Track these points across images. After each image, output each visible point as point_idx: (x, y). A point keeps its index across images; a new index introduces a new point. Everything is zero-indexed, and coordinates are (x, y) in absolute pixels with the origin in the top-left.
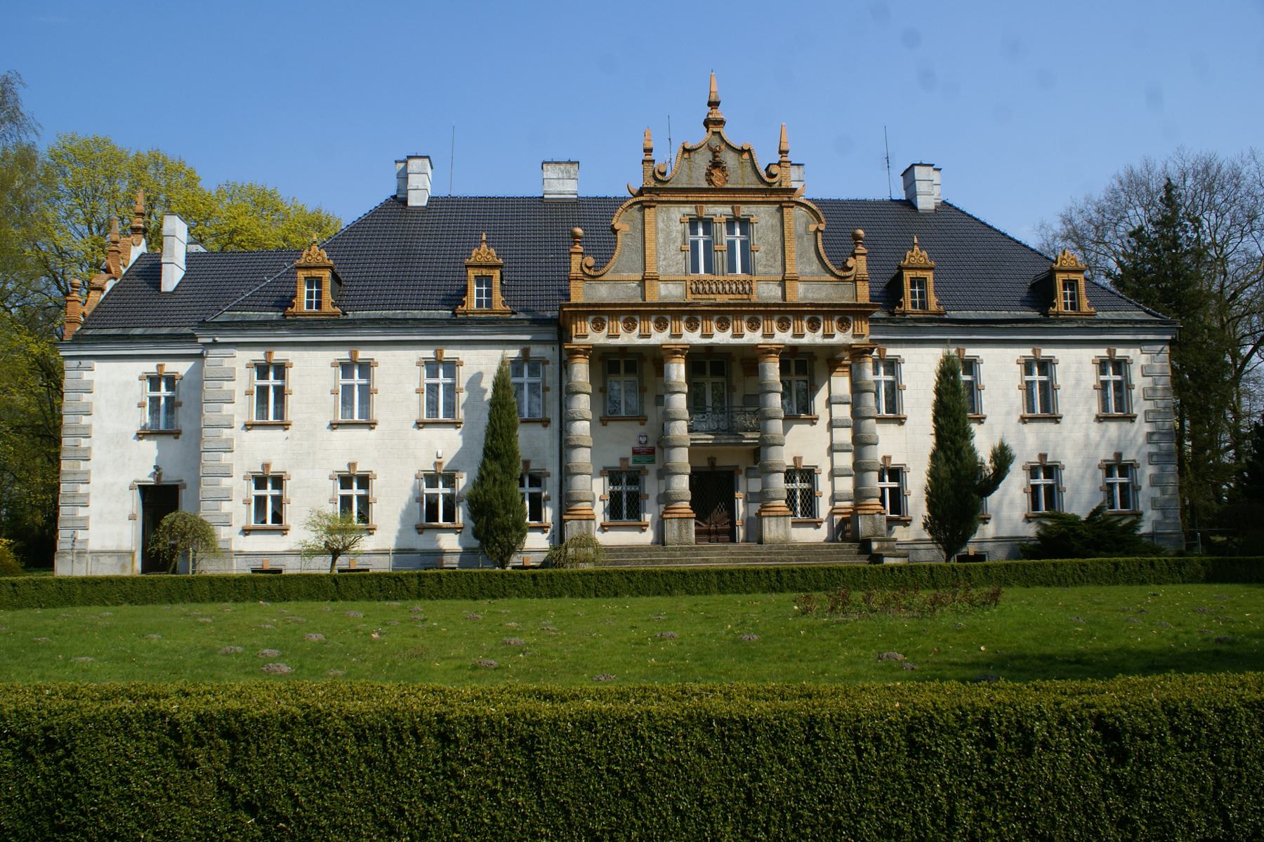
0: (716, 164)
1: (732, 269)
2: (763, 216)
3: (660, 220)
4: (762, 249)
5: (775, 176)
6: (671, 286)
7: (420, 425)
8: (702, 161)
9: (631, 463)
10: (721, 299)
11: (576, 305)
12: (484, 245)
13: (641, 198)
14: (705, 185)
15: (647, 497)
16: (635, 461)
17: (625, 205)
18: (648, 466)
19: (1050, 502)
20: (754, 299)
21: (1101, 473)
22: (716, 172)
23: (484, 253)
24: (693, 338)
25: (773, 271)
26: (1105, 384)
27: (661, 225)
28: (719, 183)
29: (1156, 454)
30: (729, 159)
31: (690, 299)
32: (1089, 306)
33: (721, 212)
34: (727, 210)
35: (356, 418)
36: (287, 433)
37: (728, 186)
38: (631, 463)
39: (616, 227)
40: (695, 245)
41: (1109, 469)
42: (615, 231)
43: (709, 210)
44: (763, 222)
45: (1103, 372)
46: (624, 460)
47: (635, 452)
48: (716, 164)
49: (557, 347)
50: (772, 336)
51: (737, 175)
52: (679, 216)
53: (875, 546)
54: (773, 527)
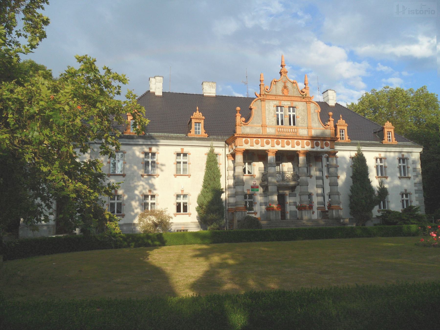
0: (285, 87)
1: (290, 124)
2: (301, 106)
3: (266, 106)
4: (300, 117)
5: (304, 92)
6: (270, 129)
7: (175, 176)
8: (280, 86)
9: (250, 191)
10: (287, 134)
11: (240, 134)
12: (198, 112)
13: (260, 98)
14: (281, 94)
15: (256, 203)
16: (252, 191)
17: (255, 100)
18: (256, 192)
19: (384, 207)
20: (298, 135)
21: (400, 196)
22: (285, 90)
23: (197, 114)
24: (279, 148)
25: (304, 125)
26: (400, 166)
27: (267, 108)
28: (286, 94)
29: (417, 190)
30: (289, 85)
31: (277, 134)
32: (395, 140)
33: (286, 104)
34: (288, 104)
35: (182, 174)
36: (124, 178)
37: (289, 95)
39: (252, 107)
40: (278, 115)
41: (402, 195)
42: (251, 109)
43: (283, 103)
44: (300, 108)
45: (400, 162)
46: (248, 190)
48: (285, 87)
49: (224, 149)
51: (292, 91)
52: (273, 105)
53: (342, 221)
54: (306, 214)
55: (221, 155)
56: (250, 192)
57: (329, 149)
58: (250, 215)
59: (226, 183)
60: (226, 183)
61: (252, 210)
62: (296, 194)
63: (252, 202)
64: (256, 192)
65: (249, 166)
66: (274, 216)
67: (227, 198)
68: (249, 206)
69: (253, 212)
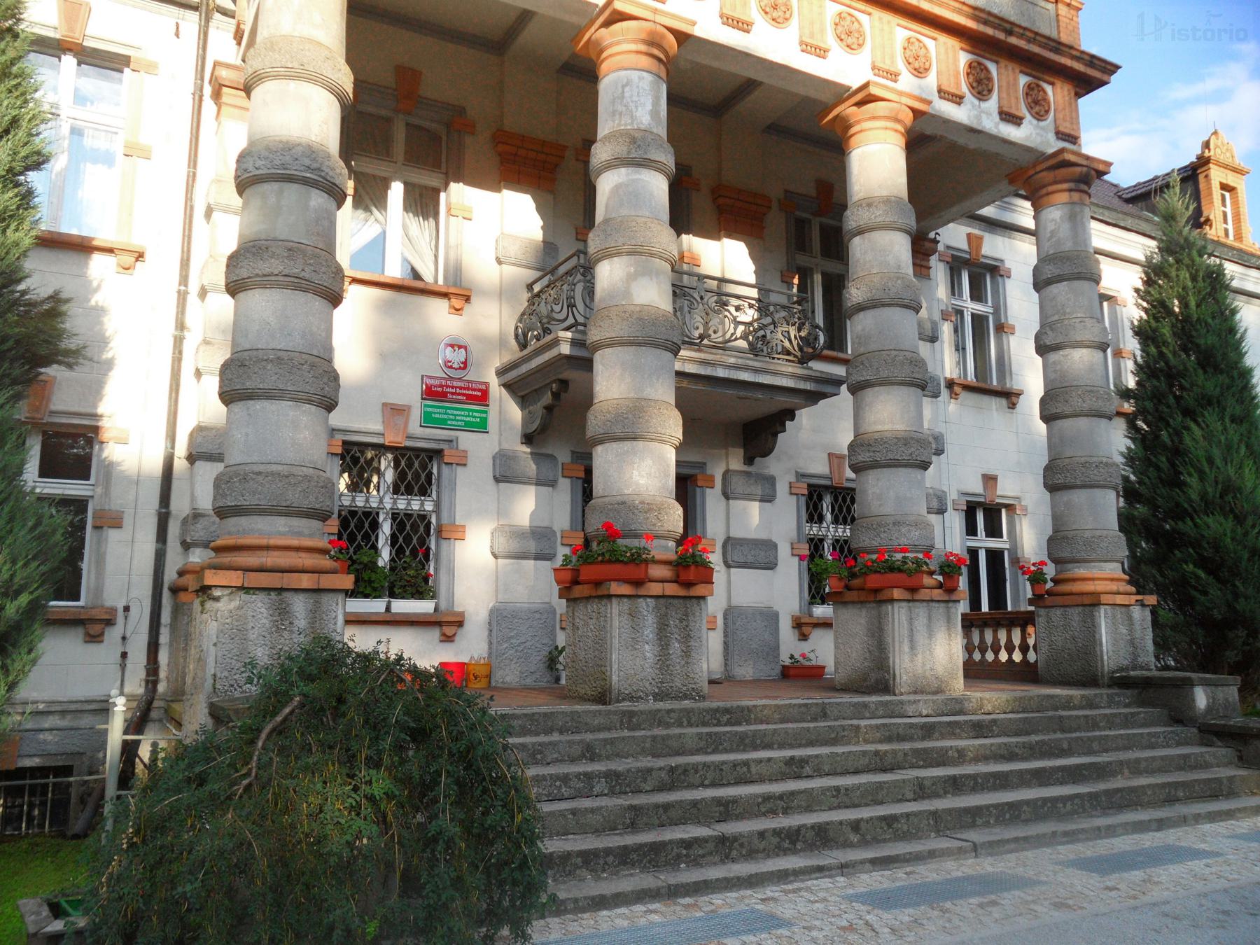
9: (415, 427)
18: (467, 441)
38: (415, 427)
46: (395, 411)
47: (431, 393)
50: (894, 76)
55: (151, 68)
56: (416, 431)
57: (1051, 136)
58: (362, 641)
59: (181, 326)
60: (181, 326)
61: (420, 589)
62: (771, 481)
63: (423, 517)
64: (467, 441)
65: (419, 228)
66: (649, 651)
67: (180, 464)
68: (398, 552)
69: (422, 607)
